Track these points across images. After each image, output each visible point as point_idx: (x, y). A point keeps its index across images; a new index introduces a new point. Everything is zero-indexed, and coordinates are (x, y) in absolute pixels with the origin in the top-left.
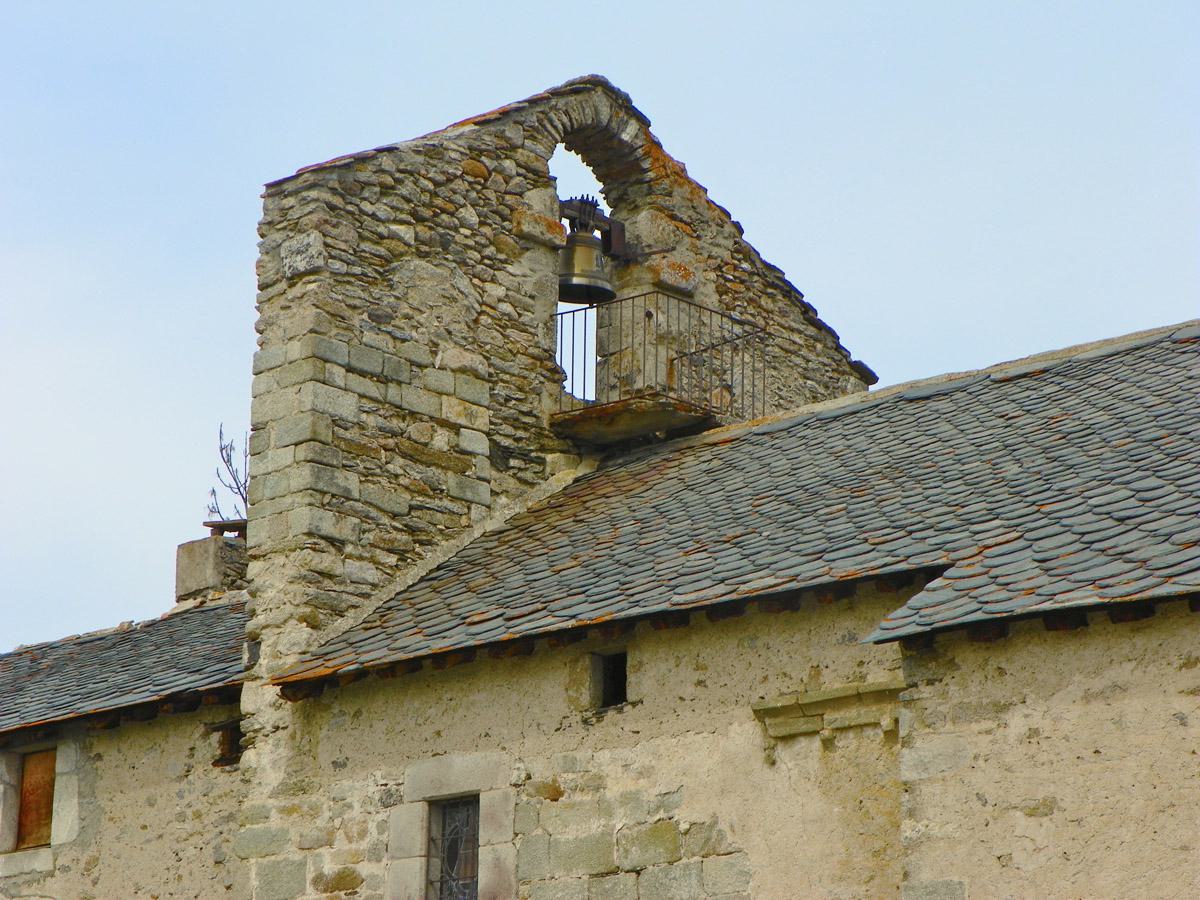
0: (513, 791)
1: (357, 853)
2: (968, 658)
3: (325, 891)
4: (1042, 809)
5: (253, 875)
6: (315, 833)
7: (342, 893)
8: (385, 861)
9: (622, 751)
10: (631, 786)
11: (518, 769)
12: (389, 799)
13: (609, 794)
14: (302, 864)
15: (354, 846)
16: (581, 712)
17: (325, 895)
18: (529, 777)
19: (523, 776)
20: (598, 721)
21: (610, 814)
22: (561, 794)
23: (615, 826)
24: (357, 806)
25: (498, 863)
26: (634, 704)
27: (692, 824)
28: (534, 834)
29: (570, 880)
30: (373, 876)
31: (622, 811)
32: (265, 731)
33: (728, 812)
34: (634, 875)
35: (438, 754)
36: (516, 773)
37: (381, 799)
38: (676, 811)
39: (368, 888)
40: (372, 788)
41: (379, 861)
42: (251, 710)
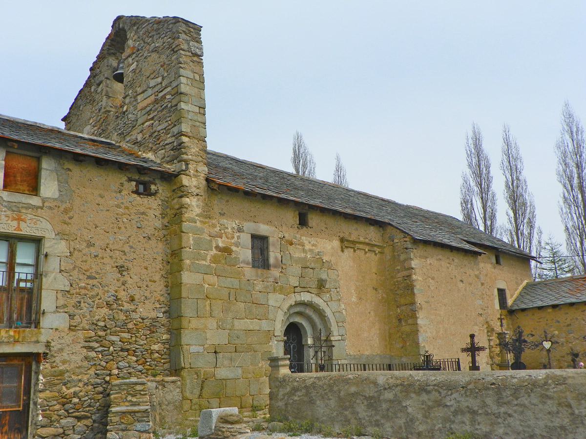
1: (231, 243)
2: (421, 246)
4: (433, 279)
5: (191, 239)
6: (215, 233)
7: (226, 254)
10: (311, 248)
12: (240, 230)
22: (293, 244)
24: (230, 229)
25: (276, 258)
33: (333, 260)
37: (237, 229)
40: (234, 225)
41: (238, 247)
42: (187, 185)
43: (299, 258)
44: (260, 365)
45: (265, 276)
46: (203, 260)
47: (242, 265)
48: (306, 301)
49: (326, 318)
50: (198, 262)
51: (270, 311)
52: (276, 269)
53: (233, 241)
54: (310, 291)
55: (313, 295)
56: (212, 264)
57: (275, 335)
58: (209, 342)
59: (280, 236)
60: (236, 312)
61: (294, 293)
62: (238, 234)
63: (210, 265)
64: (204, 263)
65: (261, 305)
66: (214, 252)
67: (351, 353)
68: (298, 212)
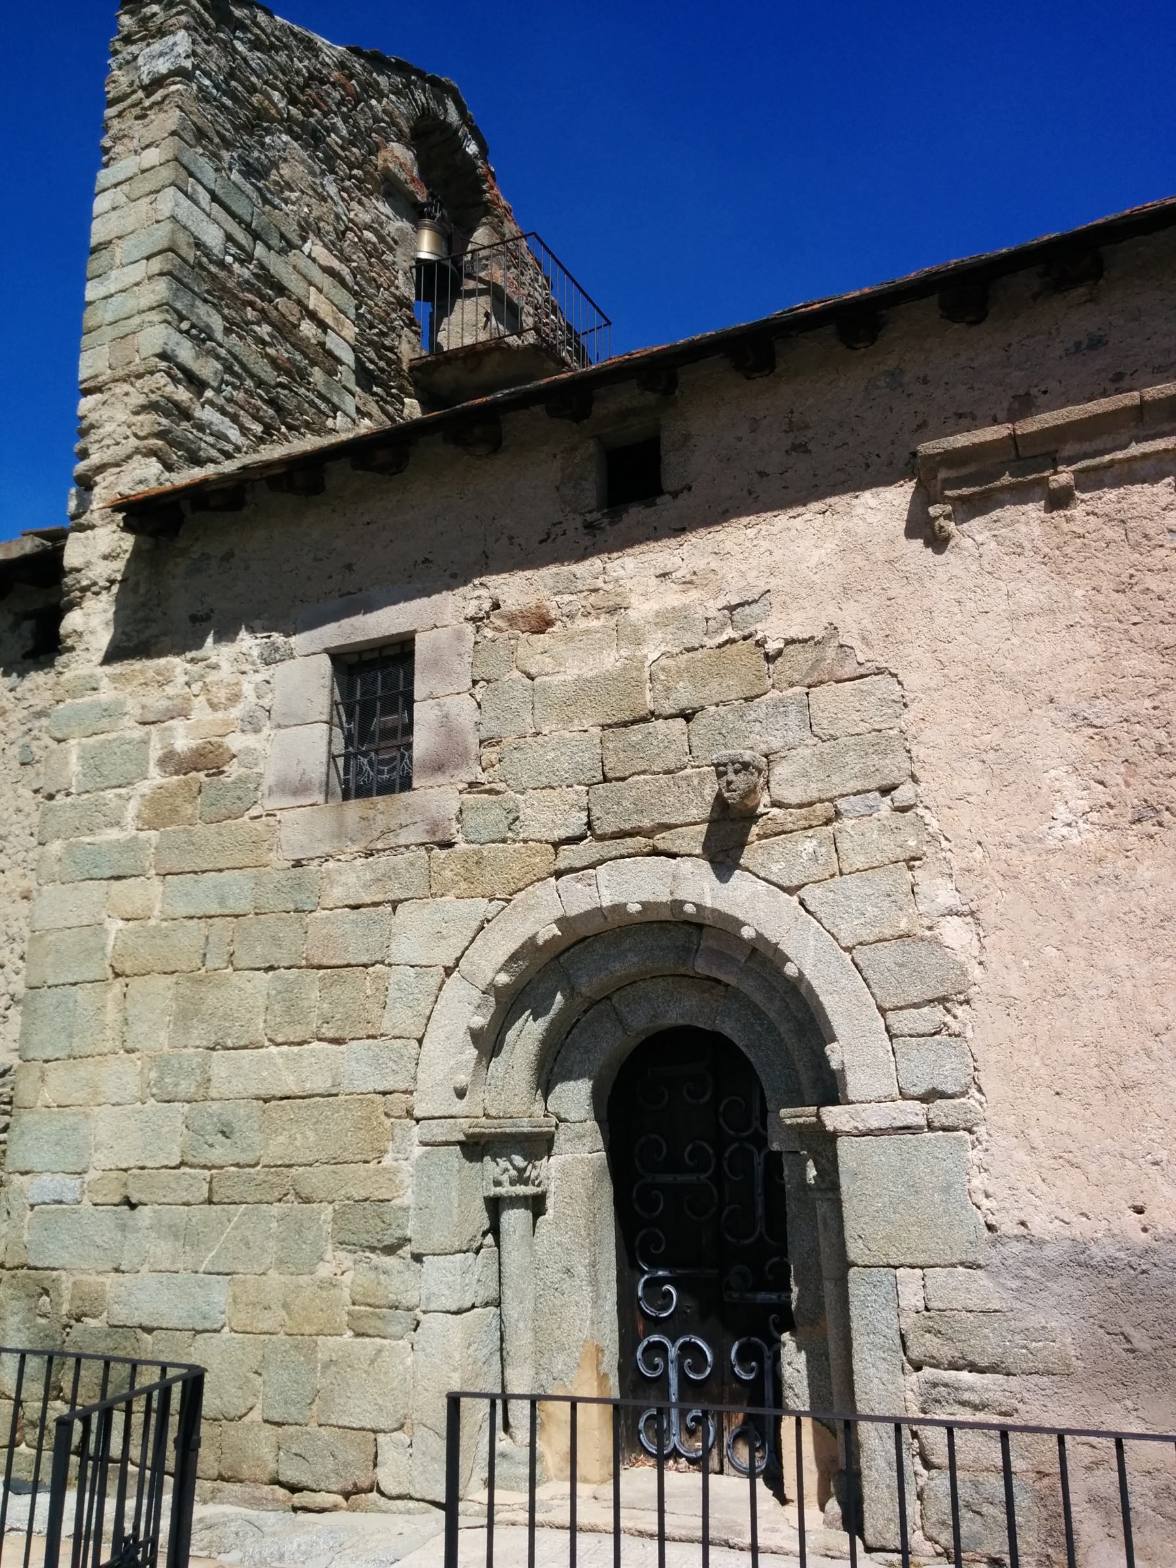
0: (470, 628)
1: (226, 723)
3: (177, 773)
5: (73, 758)
6: (166, 703)
7: (201, 775)
8: (266, 731)
11: (479, 597)
13: (633, 615)
14: (145, 742)
15: (220, 715)
16: (581, 514)
17: (175, 777)
18: (496, 606)
19: (487, 606)
20: (612, 523)
21: (638, 640)
22: (550, 623)
23: (646, 656)
24: (225, 666)
26: (675, 495)
27: (790, 642)
28: (506, 678)
29: (568, 735)
30: (249, 751)
32: (95, 589)
34: (681, 721)
35: (349, 593)
36: (475, 602)
37: (261, 655)
38: (759, 626)
39: (240, 765)
41: (257, 731)
43: (584, 686)
44: (324, 1271)
45: (381, 822)
46: (110, 825)
47: (270, 804)
50: (88, 839)
51: (393, 993)
52: (441, 779)
53: (236, 712)
54: (661, 845)
56: (142, 835)
57: (417, 1113)
58: (102, 1159)
59: (471, 611)
60: (225, 1017)
61: (558, 874)
62: (265, 673)
63: (135, 838)
64: (113, 834)
65: (344, 971)
66: (156, 778)
67: (1040, 1225)
68: (592, 446)
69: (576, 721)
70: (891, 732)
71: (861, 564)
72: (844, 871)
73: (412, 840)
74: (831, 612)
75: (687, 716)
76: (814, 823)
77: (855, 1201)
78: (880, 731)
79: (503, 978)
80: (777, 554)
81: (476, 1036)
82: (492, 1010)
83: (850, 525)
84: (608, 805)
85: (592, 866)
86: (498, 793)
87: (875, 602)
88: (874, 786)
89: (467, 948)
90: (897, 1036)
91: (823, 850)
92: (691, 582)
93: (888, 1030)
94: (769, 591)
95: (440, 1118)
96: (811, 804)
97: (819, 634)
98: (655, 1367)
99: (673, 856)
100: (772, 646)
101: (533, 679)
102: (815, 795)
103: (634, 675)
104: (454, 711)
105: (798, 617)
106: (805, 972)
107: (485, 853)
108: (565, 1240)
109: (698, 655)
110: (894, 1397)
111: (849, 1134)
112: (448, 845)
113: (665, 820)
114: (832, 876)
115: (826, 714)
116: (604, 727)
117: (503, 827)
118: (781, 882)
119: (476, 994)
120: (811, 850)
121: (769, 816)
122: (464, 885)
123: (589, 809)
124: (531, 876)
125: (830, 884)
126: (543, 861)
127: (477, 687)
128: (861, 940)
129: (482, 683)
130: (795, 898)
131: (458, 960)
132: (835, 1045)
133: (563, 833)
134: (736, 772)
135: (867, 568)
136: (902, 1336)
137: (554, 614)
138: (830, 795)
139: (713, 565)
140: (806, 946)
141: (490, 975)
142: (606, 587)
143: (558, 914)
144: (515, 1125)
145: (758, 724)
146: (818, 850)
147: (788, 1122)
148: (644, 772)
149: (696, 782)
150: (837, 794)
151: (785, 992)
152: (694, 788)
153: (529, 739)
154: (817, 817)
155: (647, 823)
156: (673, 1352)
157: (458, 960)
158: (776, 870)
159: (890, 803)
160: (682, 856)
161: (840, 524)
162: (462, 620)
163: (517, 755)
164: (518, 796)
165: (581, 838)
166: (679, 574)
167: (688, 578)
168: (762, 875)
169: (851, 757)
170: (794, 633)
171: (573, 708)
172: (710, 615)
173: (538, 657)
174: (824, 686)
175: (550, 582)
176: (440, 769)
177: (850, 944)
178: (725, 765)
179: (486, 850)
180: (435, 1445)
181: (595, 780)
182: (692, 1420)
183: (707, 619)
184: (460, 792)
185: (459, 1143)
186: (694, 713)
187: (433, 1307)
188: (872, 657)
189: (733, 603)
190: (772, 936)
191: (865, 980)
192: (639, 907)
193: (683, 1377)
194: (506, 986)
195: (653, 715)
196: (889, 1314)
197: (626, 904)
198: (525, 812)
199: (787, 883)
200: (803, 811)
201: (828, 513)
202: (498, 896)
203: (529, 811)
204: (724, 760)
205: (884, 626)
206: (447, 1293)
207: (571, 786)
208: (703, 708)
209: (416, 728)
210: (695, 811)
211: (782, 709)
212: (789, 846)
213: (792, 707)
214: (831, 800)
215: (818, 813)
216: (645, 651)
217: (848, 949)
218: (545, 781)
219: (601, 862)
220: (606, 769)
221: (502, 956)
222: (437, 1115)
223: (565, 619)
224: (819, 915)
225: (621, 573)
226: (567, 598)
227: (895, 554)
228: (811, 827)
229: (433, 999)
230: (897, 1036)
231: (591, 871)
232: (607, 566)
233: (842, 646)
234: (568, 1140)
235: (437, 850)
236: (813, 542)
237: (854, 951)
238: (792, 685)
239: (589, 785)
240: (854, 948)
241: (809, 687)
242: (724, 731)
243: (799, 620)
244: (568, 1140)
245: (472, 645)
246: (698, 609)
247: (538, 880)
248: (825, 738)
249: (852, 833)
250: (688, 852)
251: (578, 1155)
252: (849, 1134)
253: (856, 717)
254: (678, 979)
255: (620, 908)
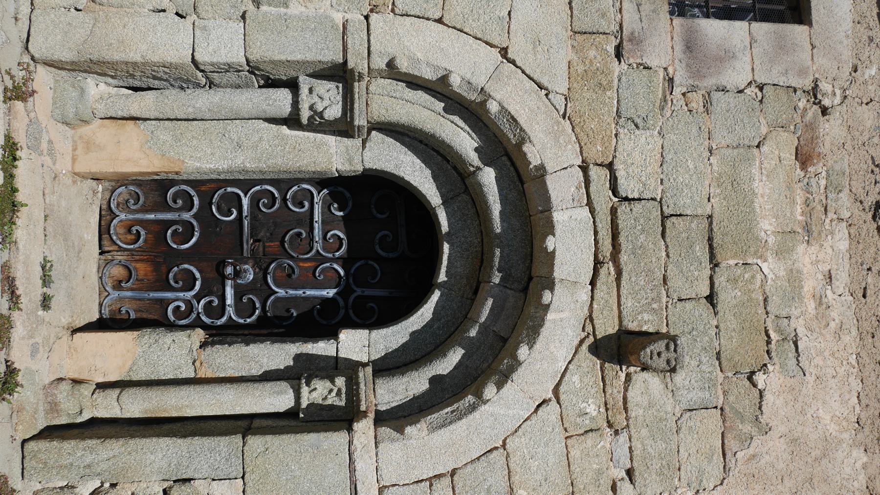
0: (808, 84)
9: (846, 269)
10: (809, 285)
11: (835, 94)
13: (801, 248)
18: (825, 111)
19: (826, 102)
21: (782, 252)
25: (726, 56)
27: (761, 393)
28: (762, 120)
29: (707, 183)
31: (782, 273)
34: (707, 292)
38: (777, 367)
48: (550, 243)
49: (470, 399)
52: (679, 48)
54: (603, 272)
55: (584, 295)
57: (374, 17)
61: (584, 168)
69: (718, 191)
70: (677, 480)
71: (813, 454)
72: (569, 441)
73: (626, 16)
74: (780, 428)
75: (711, 299)
76: (610, 413)
77: (294, 446)
78: (679, 469)
79: (493, 107)
80: (832, 383)
81: (444, 79)
82: (465, 94)
83: (844, 445)
84: (642, 221)
85: (590, 204)
86: (662, 109)
87: (781, 465)
88: (635, 465)
89: (523, 72)
90: (431, 485)
91: (587, 422)
92: (820, 304)
93: (438, 476)
94: (805, 375)
95: (369, 41)
96: (626, 409)
97: (763, 419)
98: (175, 202)
99: (593, 283)
100: (760, 378)
101: (758, 146)
102: (632, 414)
103: (752, 249)
104: (738, 65)
105: (780, 402)
106: (487, 406)
107: (608, 93)
108: (265, 145)
109: (761, 311)
110: (141, 472)
111: (350, 443)
112: (619, 55)
113: (625, 276)
114: (566, 430)
115: (698, 424)
116: (710, 217)
117: (631, 113)
118: (563, 384)
119: (480, 81)
120: (588, 411)
121: (620, 372)
122: (581, 69)
123: (640, 199)
124: (584, 139)
125: (559, 429)
126: (596, 152)
127: (757, 90)
128: (511, 456)
129: (759, 94)
130: (550, 395)
131: (513, 62)
132: (426, 432)
133: (621, 174)
134: (668, 362)
135: (809, 460)
136: (189, 480)
137: (811, 169)
138: (632, 426)
139: (833, 325)
140: (509, 408)
141: (498, 97)
142: (828, 221)
143: (549, 168)
144: (361, 112)
145: (697, 363)
146: (588, 417)
147: (361, 375)
148: (668, 256)
149: (655, 306)
150: (632, 433)
151: (467, 366)
152: (649, 304)
153: (706, 143)
154: (615, 415)
155: (624, 258)
156: (187, 216)
157: (513, 62)
158: (574, 380)
159: (620, 477)
160: (592, 291)
161: (845, 436)
162: (817, 76)
163: (694, 130)
164: (658, 128)
165: (615, 192)
166: (829, 293)
167: (824, 300)
168: (571, 367)
169: (662, 445)
170: (769, 397)
171: (730, 188)
172: (793, 320)
173: (777, 152)
174: (721, 423)
175: (837, 167)
176: (688, 48)
177: (508, 446)
178: (675, 351)
179: (612, 94)
180: (78, 36)
181: (665, 208)
182: (137, 230)
183: (788, 318)
184: (666, 69)
185: (345, 63)
186: (714, 306)
187: (198, 32)
188: (739, 463)
189: (799, 343)
190: (519, 376)
191: (478, 458)
192: (550, 249)
193: (167, 224)
194: (487, 111)
195: (715, 264)
196: (205, 471)
197: (554, 235)
198: (642, 136)
199: (562, 389)
200: (621, 403)
201: (857, 425)
202: (569, 105)
203: (643, 140)
204: (679, 350)
205: (762, 473)
206: (210, 49)
207: (662, 183)
208: (716, 314)
209: (725, 23)
210: (629, 305)
211: (707, 386)
212: (593, 391)
213: (708, 396)
214: (628, 426)
215: (618, 417)
216: (770, 260)
217: (504, 445)
218: (668, 158)
219: (592, 211)
220: (674, 219)
221: (513, 109)
222: (372, 38)
223: (806, 180)
224: (534, 418)
225: (837, 237)
226: (823, 182)
227: (816, 483)
228: (607, 410)
229: (479, 36)
230: (431, 485)
231: (585, 201)
232: (844, 224)
233: (752, 438)
234: (347, 150)
235: (614, 42)
236: (837, 413)
237: (502, 450)
238: (725, 393)
239: (660, 202)
240: (505, 449)
241: (722, 409)
242: (694, 333)
243: (777, 402)
244: (347, 150)
245: (793, 85)
246: (799, 310)
247: (581, 148)
248: (679, 422)
249: (599, 447)
250: (595, 298)
251: (334, 159)
252: (350, 443)
253: (693, 450)
254: (480, 255)
255: (550, 228)
